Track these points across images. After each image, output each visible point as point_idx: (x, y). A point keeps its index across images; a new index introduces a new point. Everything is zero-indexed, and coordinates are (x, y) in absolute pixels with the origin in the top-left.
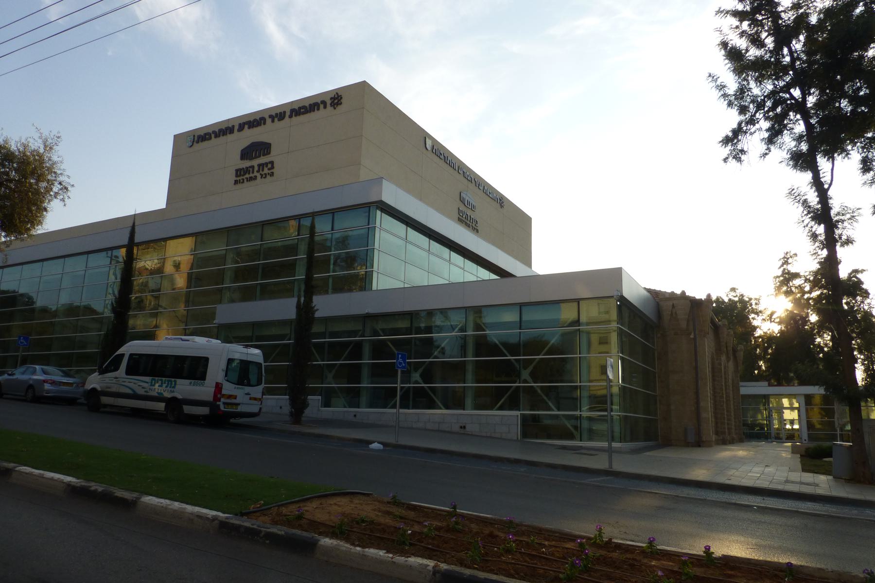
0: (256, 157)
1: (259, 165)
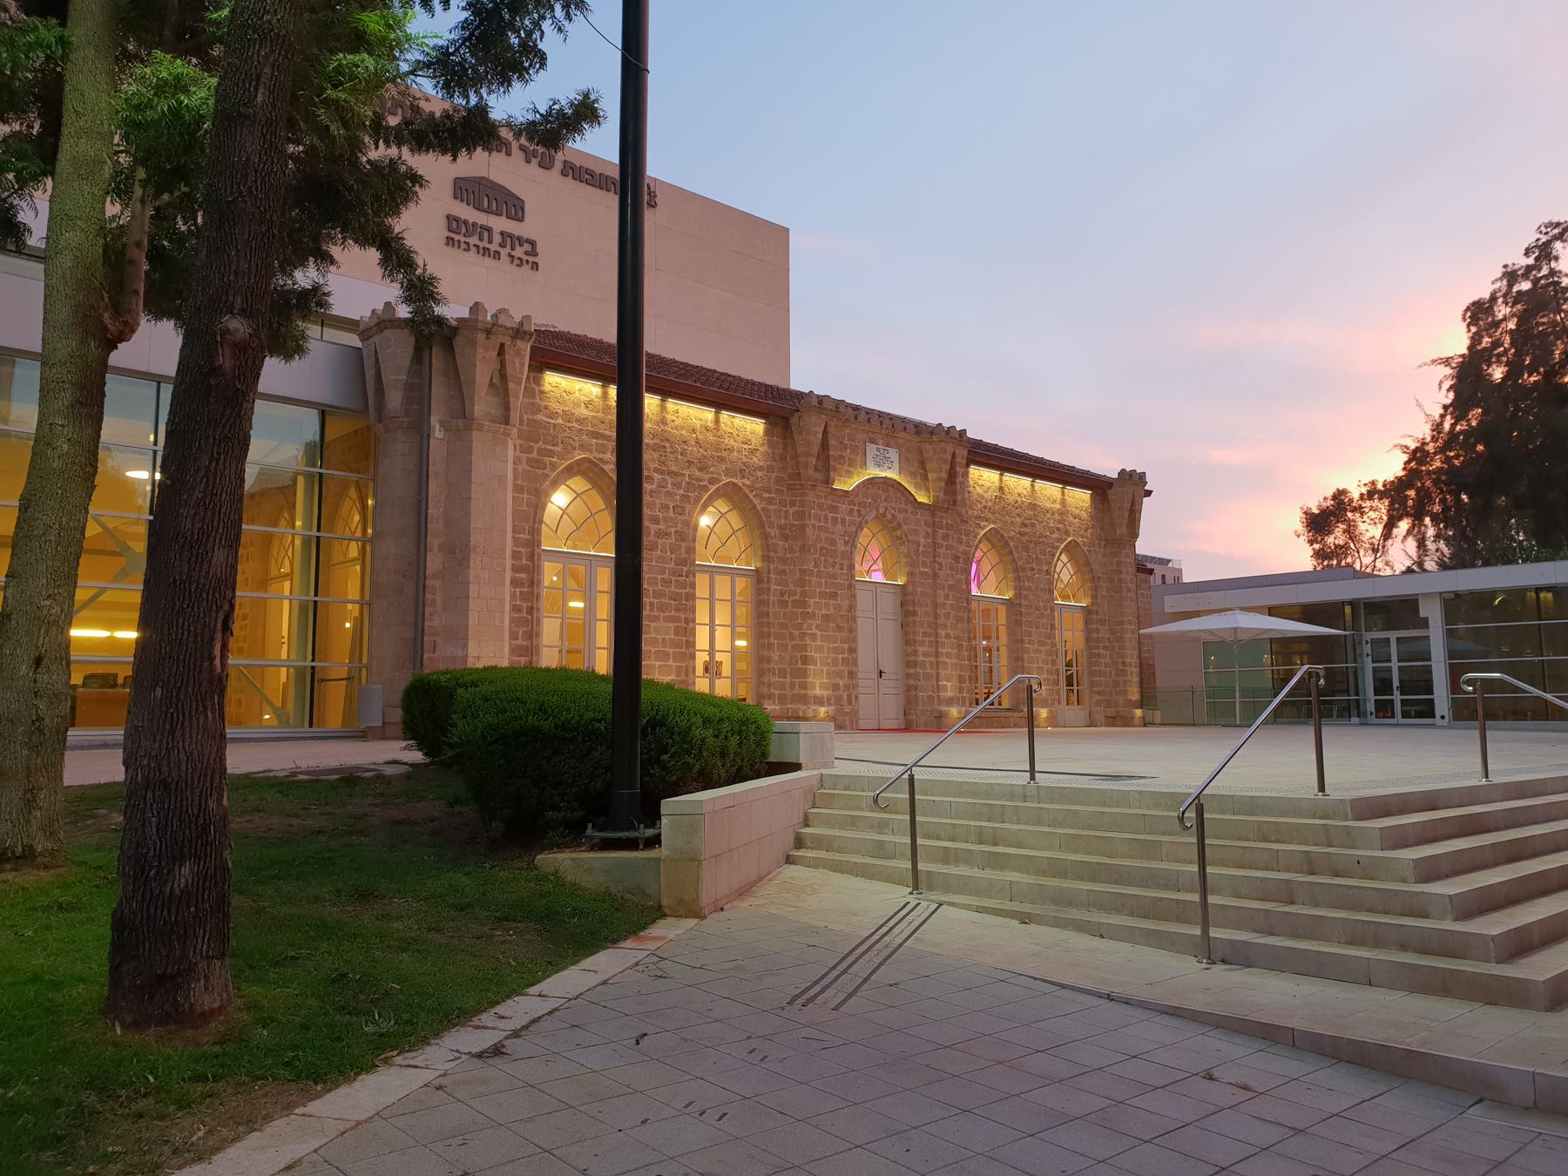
0: (488, 211)
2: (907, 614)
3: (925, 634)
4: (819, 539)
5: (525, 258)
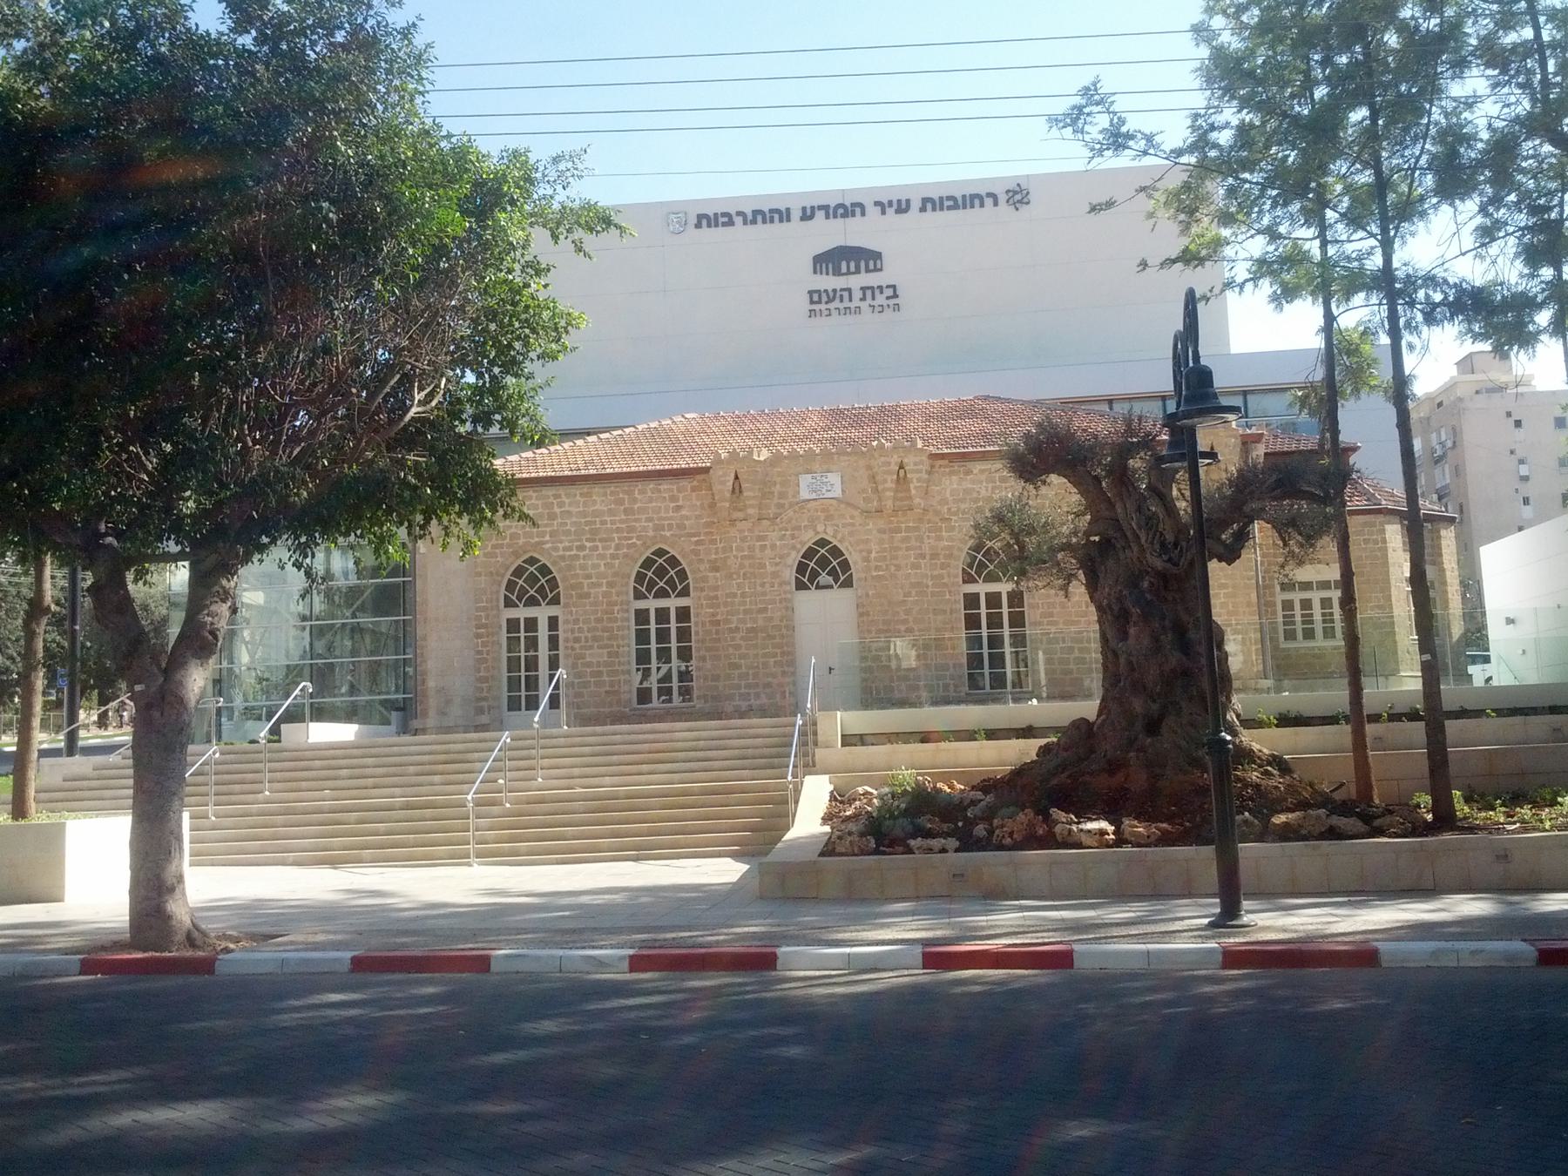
0: (849, 273)
2: (861, 615)
3: (879, 631)
4: (742, 566)
5: (885, 303)
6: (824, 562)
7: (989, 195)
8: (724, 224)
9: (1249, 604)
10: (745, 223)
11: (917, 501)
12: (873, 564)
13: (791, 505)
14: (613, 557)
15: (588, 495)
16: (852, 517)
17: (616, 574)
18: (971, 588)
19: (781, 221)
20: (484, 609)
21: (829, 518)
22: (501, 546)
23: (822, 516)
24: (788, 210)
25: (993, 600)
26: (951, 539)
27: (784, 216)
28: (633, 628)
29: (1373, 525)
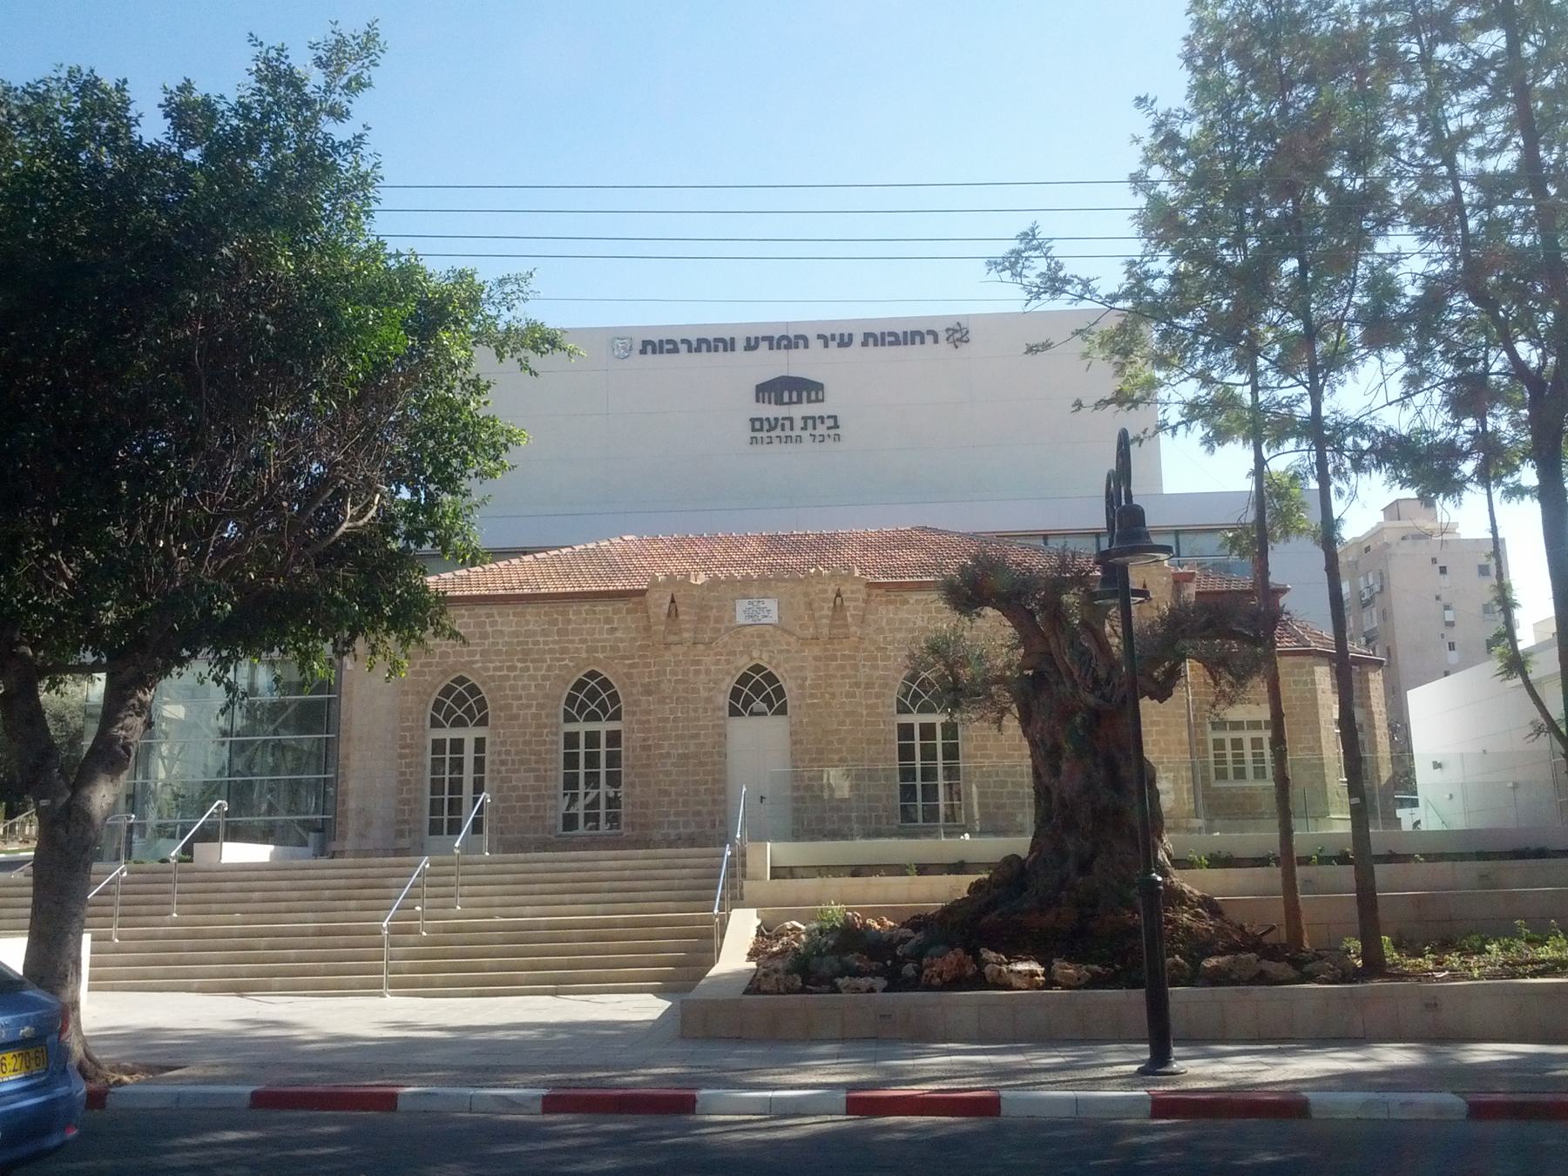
0: (791, 402)
1: (805, 419)
2: (795, 743)
3: (812, 760)
5: (826, 433)
6: (757, 689)
7: (930, 332)
8: (669, 351)
9: (1180, 742)
10: (690, 351)
11: (853, 629)
12: (808, 691)
13: (728, 630)
14: (545, 678)
15: (522, 614)
16: (788, 644)
17: (546, 696)
18: (905, 719)
19: (725, 350)
20: (410, 729)
21: (765, 644)
22: (429, 665)
23: (758, 641)
24: (732, 339)
25: (928, 731)
26: (886, 668)
27: (728, 345)
28: (562, 750)
29: (1301, 666)
